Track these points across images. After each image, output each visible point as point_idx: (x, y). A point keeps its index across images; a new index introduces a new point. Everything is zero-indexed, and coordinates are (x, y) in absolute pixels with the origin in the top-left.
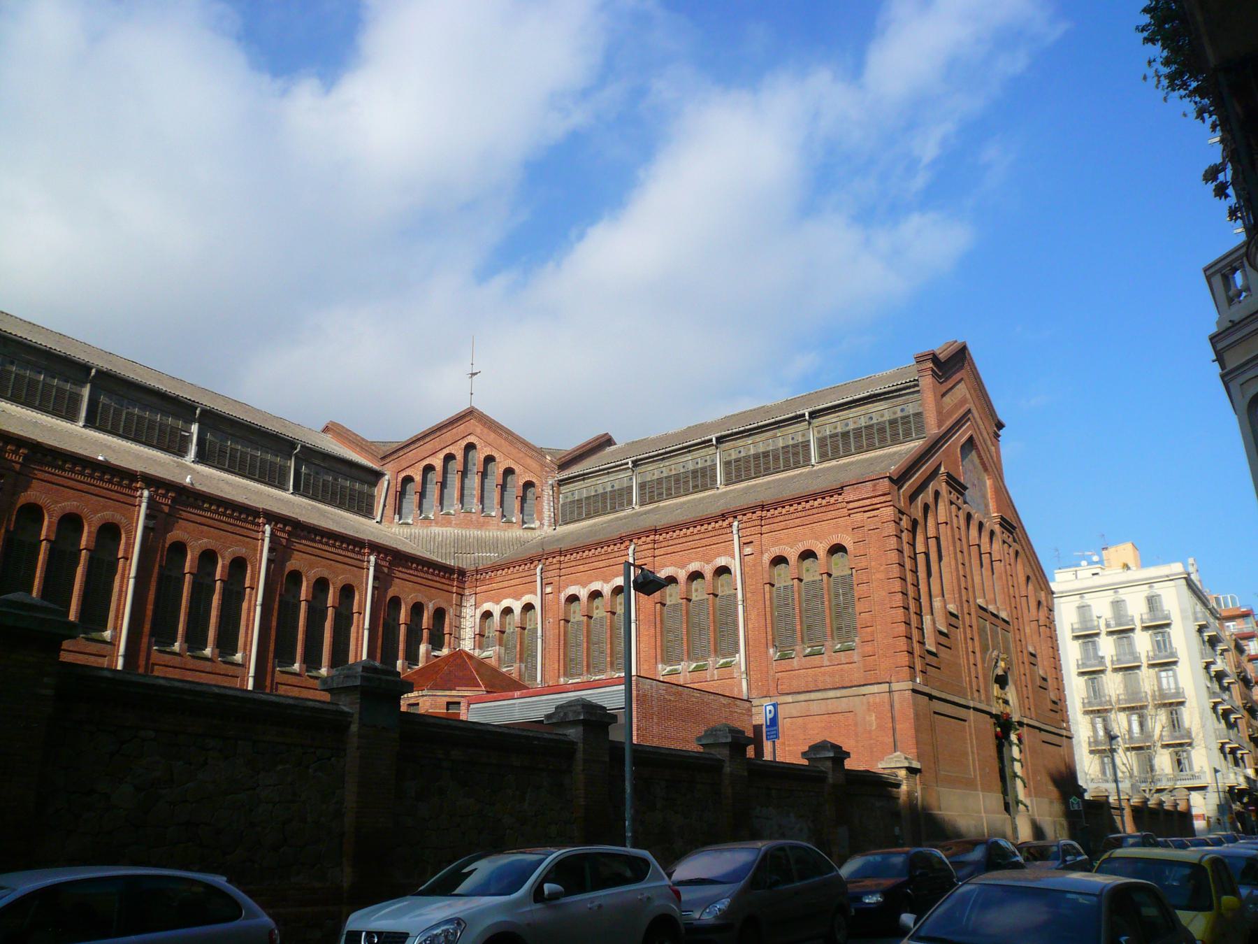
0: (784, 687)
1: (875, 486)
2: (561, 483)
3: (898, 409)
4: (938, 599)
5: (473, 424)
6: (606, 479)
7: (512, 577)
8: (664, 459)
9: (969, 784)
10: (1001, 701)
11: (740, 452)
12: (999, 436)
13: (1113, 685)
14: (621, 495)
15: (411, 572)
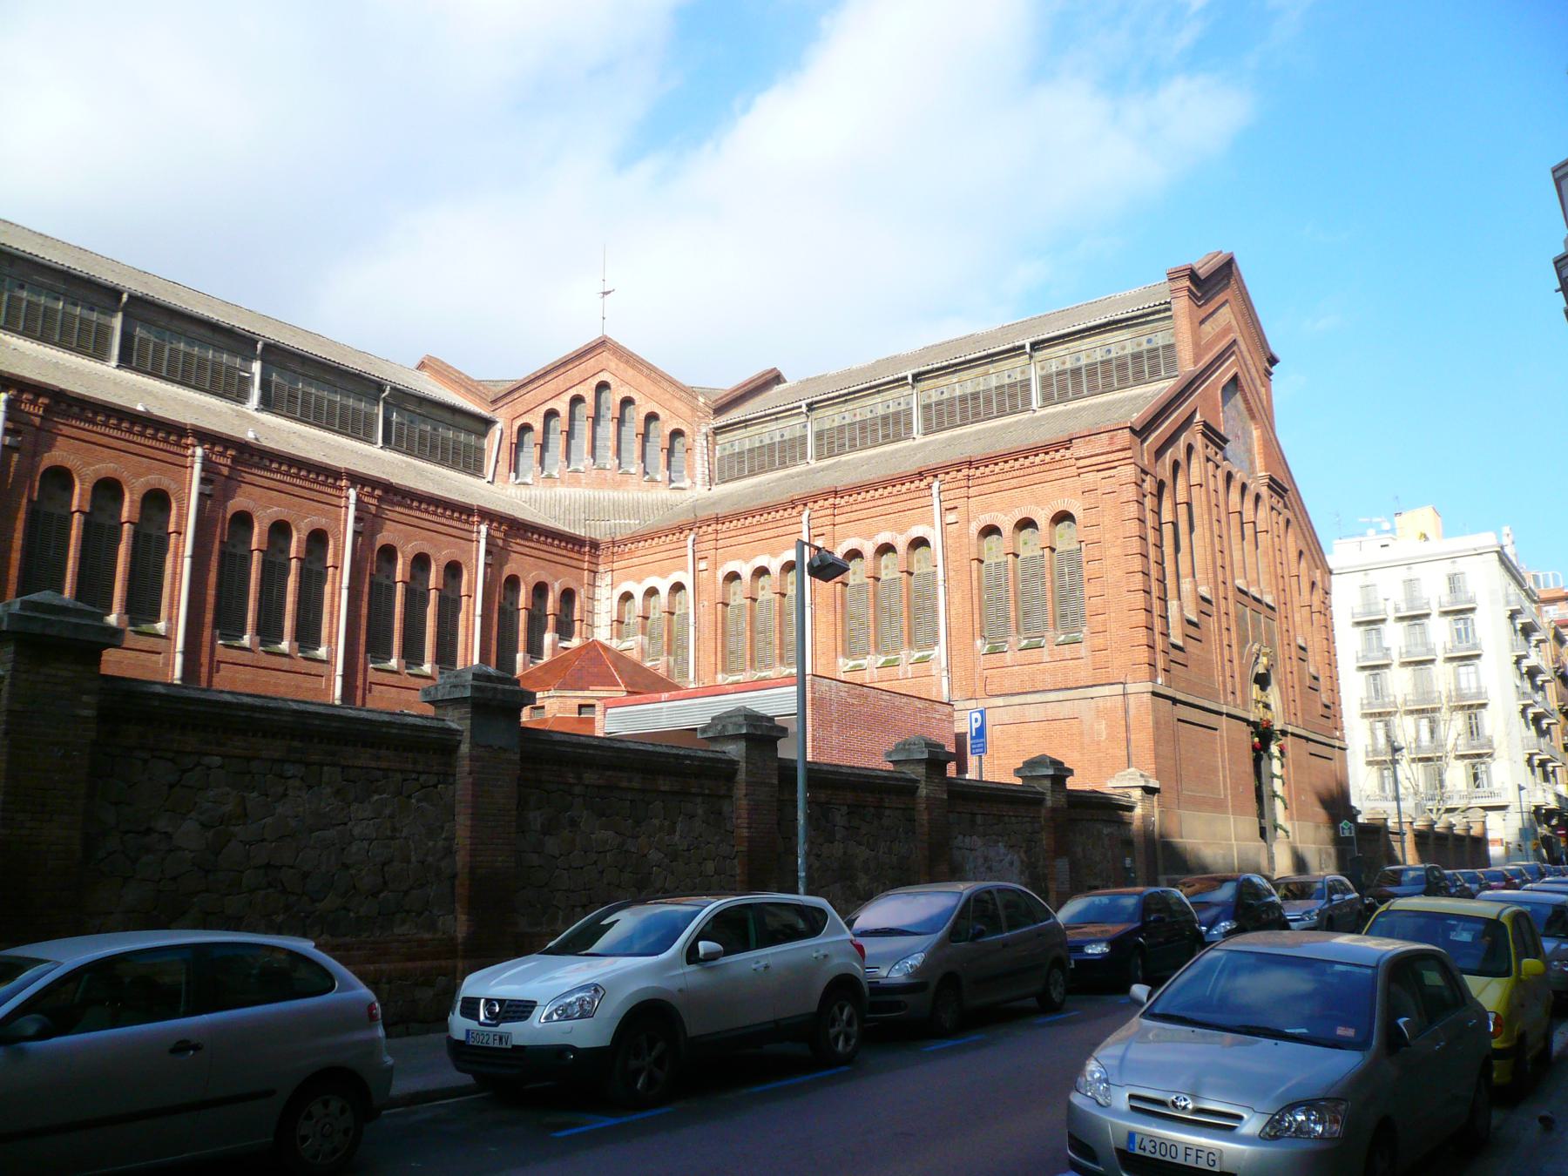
1: (1112, 438)
2: (718, 431)
3: (1145, 339)
5: (605, 358)
6: (773, 426)
7: (658, 549)
8: (846, 401)
9: (1218, 806)
10: (1260, 705)
11: (942, 393)
12: (1271, 374)
13: (1399, 683)
14: (793, 447)
15: (532, 544)
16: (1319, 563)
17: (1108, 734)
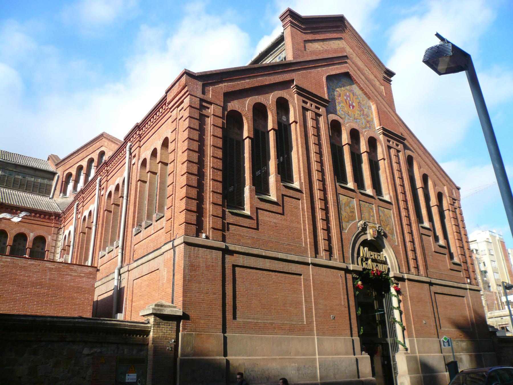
0: (136, 257)
4: (272, 176)
10: (370, 261)
12: (391, 81)
17: (167, 277)
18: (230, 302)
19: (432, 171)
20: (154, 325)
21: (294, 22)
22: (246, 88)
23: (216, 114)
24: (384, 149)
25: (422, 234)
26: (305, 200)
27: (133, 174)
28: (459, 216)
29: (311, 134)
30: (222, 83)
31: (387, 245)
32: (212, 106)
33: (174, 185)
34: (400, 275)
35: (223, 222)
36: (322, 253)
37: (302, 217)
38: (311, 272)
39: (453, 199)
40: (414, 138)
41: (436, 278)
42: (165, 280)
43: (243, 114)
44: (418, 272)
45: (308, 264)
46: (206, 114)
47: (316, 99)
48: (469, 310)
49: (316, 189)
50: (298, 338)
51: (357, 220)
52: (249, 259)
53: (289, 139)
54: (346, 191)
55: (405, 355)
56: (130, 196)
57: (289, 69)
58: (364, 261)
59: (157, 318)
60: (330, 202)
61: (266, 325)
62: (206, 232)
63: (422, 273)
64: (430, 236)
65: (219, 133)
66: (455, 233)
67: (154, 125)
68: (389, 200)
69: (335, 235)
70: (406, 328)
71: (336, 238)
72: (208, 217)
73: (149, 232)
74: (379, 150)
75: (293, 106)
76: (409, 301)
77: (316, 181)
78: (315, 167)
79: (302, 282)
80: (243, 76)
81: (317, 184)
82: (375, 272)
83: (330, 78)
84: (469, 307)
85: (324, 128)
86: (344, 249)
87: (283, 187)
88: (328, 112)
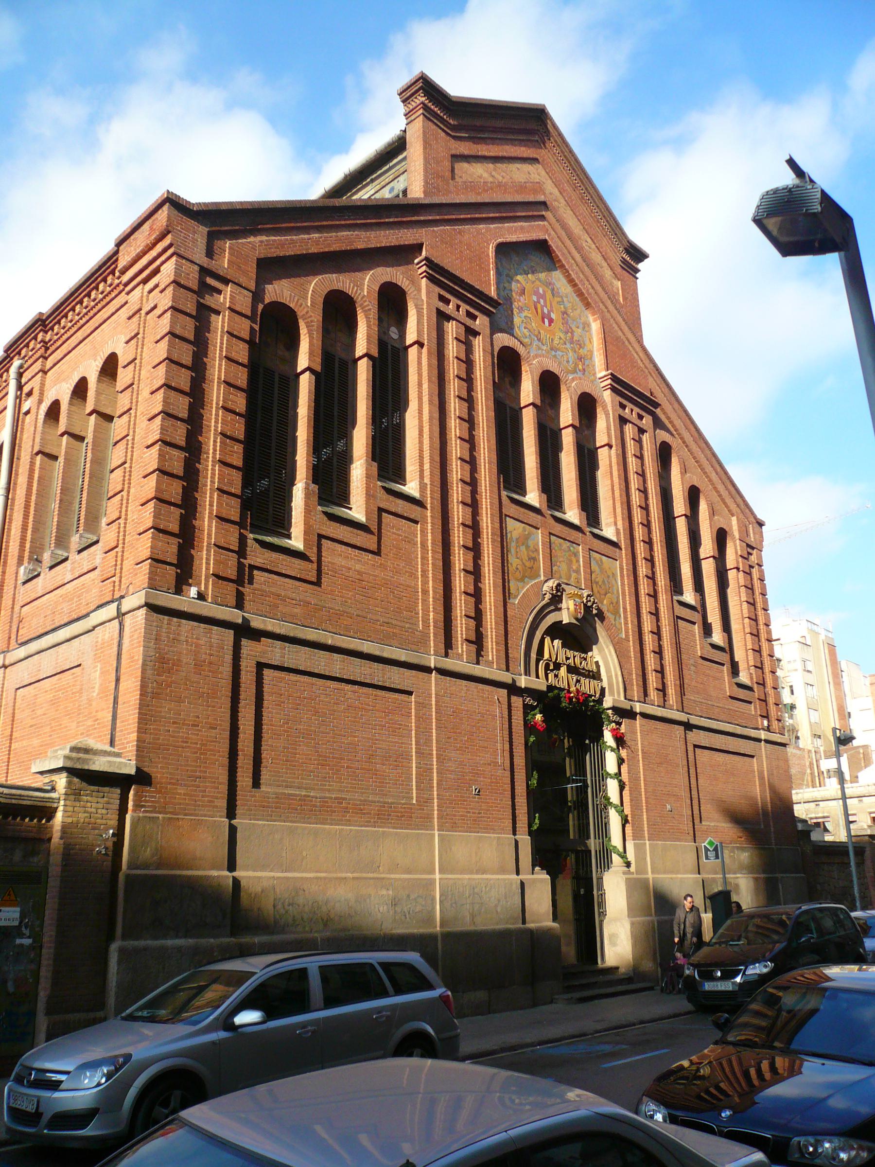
0: (24, 635)
10: (563, 671)
16: (733, 507)
17: (101, 685)
18: (248, 747)
19: (710, 480)
20: (65, 794)
21: (432, 107)
22: (310, 251)
23: (238, 309)
24: (612, 424)
25: (678, 617)
26: (429, 525)
27: (25, 436)
28: (757, 583)
29: (452, 375)
30: (255, 236)
31: (603, 637)
32: (229, 289)
33: (128, 470)
34: (626, 705)
35: (239, 563)
36: (460, 646)
37: (420, 563)
38: (433, 688)
39: (748, 546)
40: (676, 405)
41: (700, 714)
42: (97, 691)
43: (300, 313)
44: (665, 701)
45: (427, 670)
46: (213, 306)
47: (469, 295)
48: (762, 784)
49: (455, 501)
50: (396, 834)
51: (542, 578)
52: (297, 652)
53: (402, 383)
54: (523, 510)
55: (624, 877)
56: (15, 490)
57: (413, 219)
58: (552, 671)
59: (76, 780)
60: (485, 534)
61: (327, 802)
62: (198, 584)
63: (671, 703)
64: (694, 623)
65: (242, 353)
66: (747, 621)
67: (82, 322)
68: (614, 539)
69: (491, 609)
70: (629, 818)
71: (493, 614)
72: (205, 548)
73: (59, 578)
74: (601, 424)
75: (416, 306)
76: (641, 762)
77: (457, 484)
78: (456, 450)
79: (413, 710)
80: (306, 224)
81: (460, 489)
82: (572, 695)
83: (503, 249)
84: (761, 778)
85: (482, 363)
86: (509, 642)
87: (383, 491)
88: (495, 329)
